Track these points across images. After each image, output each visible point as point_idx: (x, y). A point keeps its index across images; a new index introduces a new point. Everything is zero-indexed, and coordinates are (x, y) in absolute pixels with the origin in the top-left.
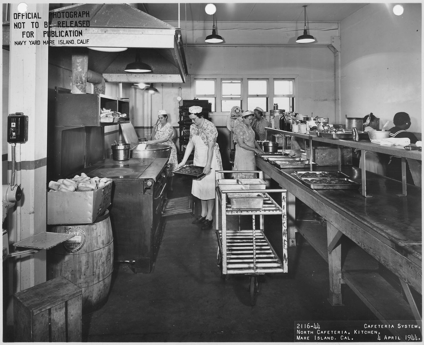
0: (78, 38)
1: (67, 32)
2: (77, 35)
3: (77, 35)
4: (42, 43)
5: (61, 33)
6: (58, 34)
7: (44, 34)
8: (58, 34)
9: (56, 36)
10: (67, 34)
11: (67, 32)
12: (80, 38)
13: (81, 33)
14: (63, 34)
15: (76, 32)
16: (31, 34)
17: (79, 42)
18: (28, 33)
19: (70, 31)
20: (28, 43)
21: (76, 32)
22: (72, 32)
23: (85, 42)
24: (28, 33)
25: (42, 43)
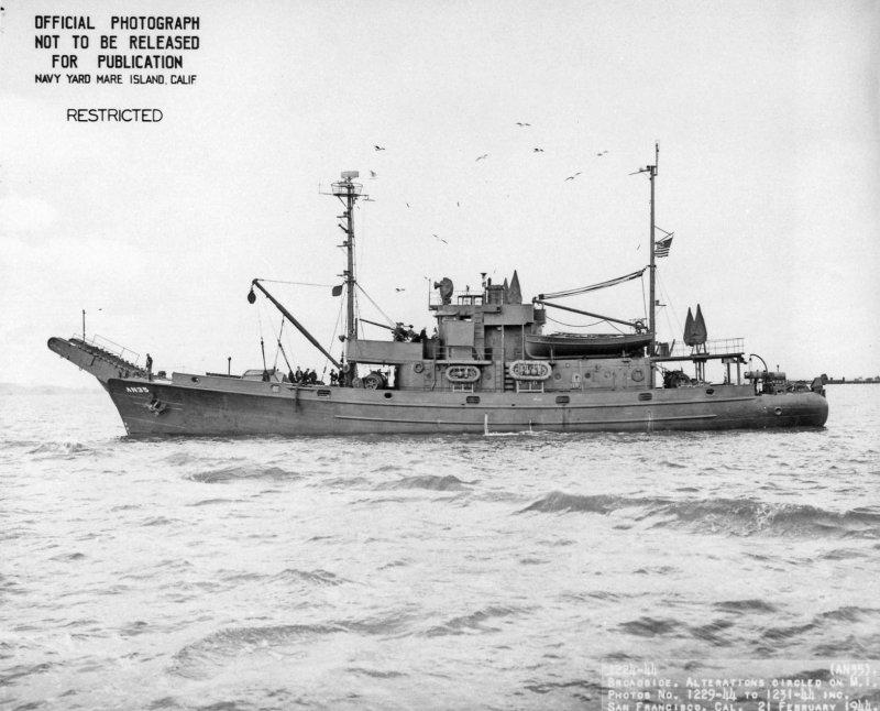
0: (173, 71)
1: (148, 58)
2: (170, 65)
3: (170, 65)
4: (94, 78)
5: (135, 59)
6: (129, 63)
7: (100, 61)
8: (129, 63)
9: (125, 67)
11: (148, 58)
12: (178, 71)
13: (178, 62)
14: (142, 62)
15: (170, 60)
16: (72, 61)
17: (175, 80)
18: (65, 59)
19: (157, 57)
20: (64, 79)
21: (170, 60)
22: (160, 60)
23: (187, 81)
24: (65, 59)
25: (94, 78)
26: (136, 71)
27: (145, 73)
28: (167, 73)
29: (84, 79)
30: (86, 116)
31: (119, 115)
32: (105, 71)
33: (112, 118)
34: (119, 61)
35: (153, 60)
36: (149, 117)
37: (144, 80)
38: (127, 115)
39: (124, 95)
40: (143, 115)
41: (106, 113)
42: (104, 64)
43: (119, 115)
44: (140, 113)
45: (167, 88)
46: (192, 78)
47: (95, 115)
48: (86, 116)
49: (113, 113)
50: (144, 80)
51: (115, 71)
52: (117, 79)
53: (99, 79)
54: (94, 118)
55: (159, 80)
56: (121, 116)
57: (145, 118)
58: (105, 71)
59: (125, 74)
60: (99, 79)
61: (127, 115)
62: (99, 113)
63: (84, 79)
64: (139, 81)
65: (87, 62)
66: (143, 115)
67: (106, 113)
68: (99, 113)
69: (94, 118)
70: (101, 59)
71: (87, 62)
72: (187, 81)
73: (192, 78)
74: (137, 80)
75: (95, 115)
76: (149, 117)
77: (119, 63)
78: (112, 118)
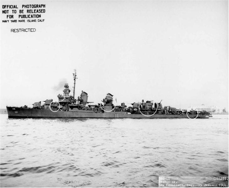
0: (38, 18)
1: (32, 15)
4: (18, 21)
6: (27, 17)
7: (19, 16)
8: (27, 17)
9: (26, 18)
10: (32, 16)
11: (32, 15)
12: (40, 18)
13: (40, 16)
14: (30, 16)
15: (37, 16)
17: (39, 21)
19: (34, 15)
21: (37, 16)
22: (35, 16)
23: (42, 21)
25: (18, 21)
26: (28, 19)
28: (37, 19)
29: (15, 21)
31: (24, 30)
32: (21, 19)
33: (23, 31)
34: (24, 16)
35: (33, 16)
37: (31, 21)
38: (26, 30)
39: (26, 25)
40: (31, 30)
41: (21, 30)
43: (24, 30)
44: (30, 30)
45: (37, 23)
46: (43, 20)
48: (16, 31)
50: (31, 21)
51: (23, 19)
52: (24, 21)
53: (19, 21)
54: (18, 31)
55: (35, 21)
57: (31, 31)
58: (21, 19)
59: (26, 19)
60: (19, 21)
61: (26, 30)
63: (15, 21)
64: (30, 21)
65: (16, 17)
66: (31, 30)
68: (19, 30)
69: (18, 31)
70: (19, 16)
71: (16, 17)
73: (43, 20)
74: (29, 21)
76: (32, 30)
78: (23, 31)
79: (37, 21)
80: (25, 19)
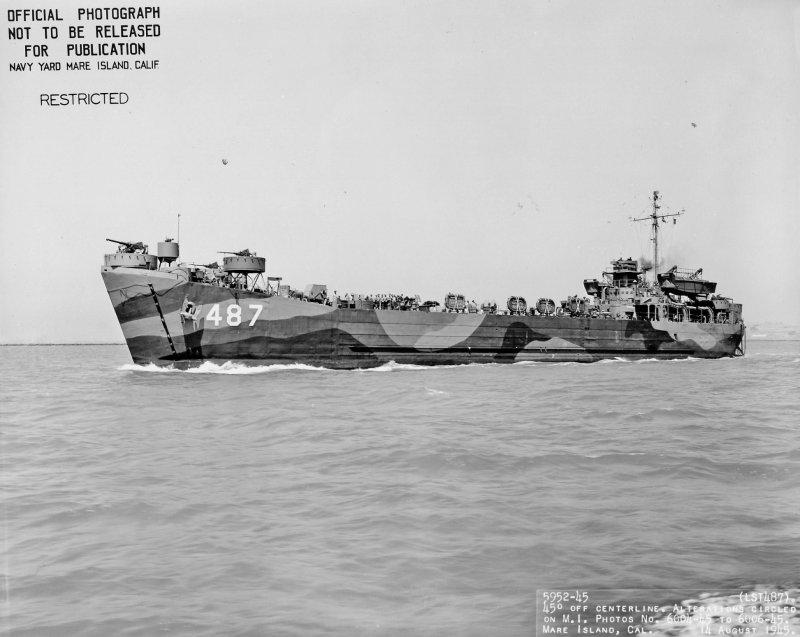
2: (134, 51)
3: (134, 51)
9: (93, 54)
12: (141, 57)
17: (139, 65)
23: (150, 65)
26: (102, 58)
27: (111, 59)
28: (131, 59)
29: (55, 66)
30: (58, 100)
31: (88, 99)
32: (74, 58)
36: (117, 100)
37: (110, 66)
38: (96, 99)
39: (93, 79)
40: (110, 97)
41: (76, 97)
42: (73, 52)
43: (88, 99)
44: (107, 96)
45: (132, 71)
46: (155, 63)
47: (66, 99)
48: (58, 100)
49: (82, 97)
50: (110, 66)
51: (83, 58)
52: (85, 66)
54: (65, 102)
55: (124, 65)
56: (90, 99)
58: (74, 58)
59: (93, 60)
61: (96, 99)
62: (70, 98)
63: (55, 66)
66: (110, 97)
67: (76, 97)
68: (70, 98)
69: (65, 102)
72: (150, 65)
73: (155, 63)
74: (104, 66)
75: (66, 99)
76: (116, 99)
77: (87, 52)
79: (132, 65)
80: (89, 58)
